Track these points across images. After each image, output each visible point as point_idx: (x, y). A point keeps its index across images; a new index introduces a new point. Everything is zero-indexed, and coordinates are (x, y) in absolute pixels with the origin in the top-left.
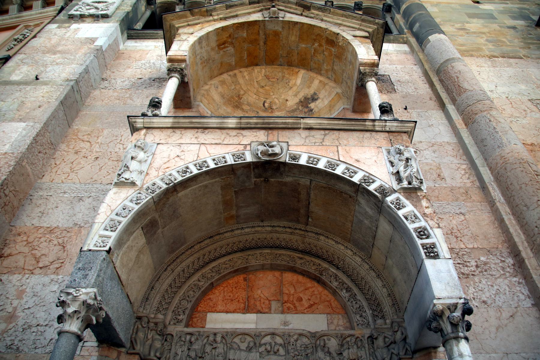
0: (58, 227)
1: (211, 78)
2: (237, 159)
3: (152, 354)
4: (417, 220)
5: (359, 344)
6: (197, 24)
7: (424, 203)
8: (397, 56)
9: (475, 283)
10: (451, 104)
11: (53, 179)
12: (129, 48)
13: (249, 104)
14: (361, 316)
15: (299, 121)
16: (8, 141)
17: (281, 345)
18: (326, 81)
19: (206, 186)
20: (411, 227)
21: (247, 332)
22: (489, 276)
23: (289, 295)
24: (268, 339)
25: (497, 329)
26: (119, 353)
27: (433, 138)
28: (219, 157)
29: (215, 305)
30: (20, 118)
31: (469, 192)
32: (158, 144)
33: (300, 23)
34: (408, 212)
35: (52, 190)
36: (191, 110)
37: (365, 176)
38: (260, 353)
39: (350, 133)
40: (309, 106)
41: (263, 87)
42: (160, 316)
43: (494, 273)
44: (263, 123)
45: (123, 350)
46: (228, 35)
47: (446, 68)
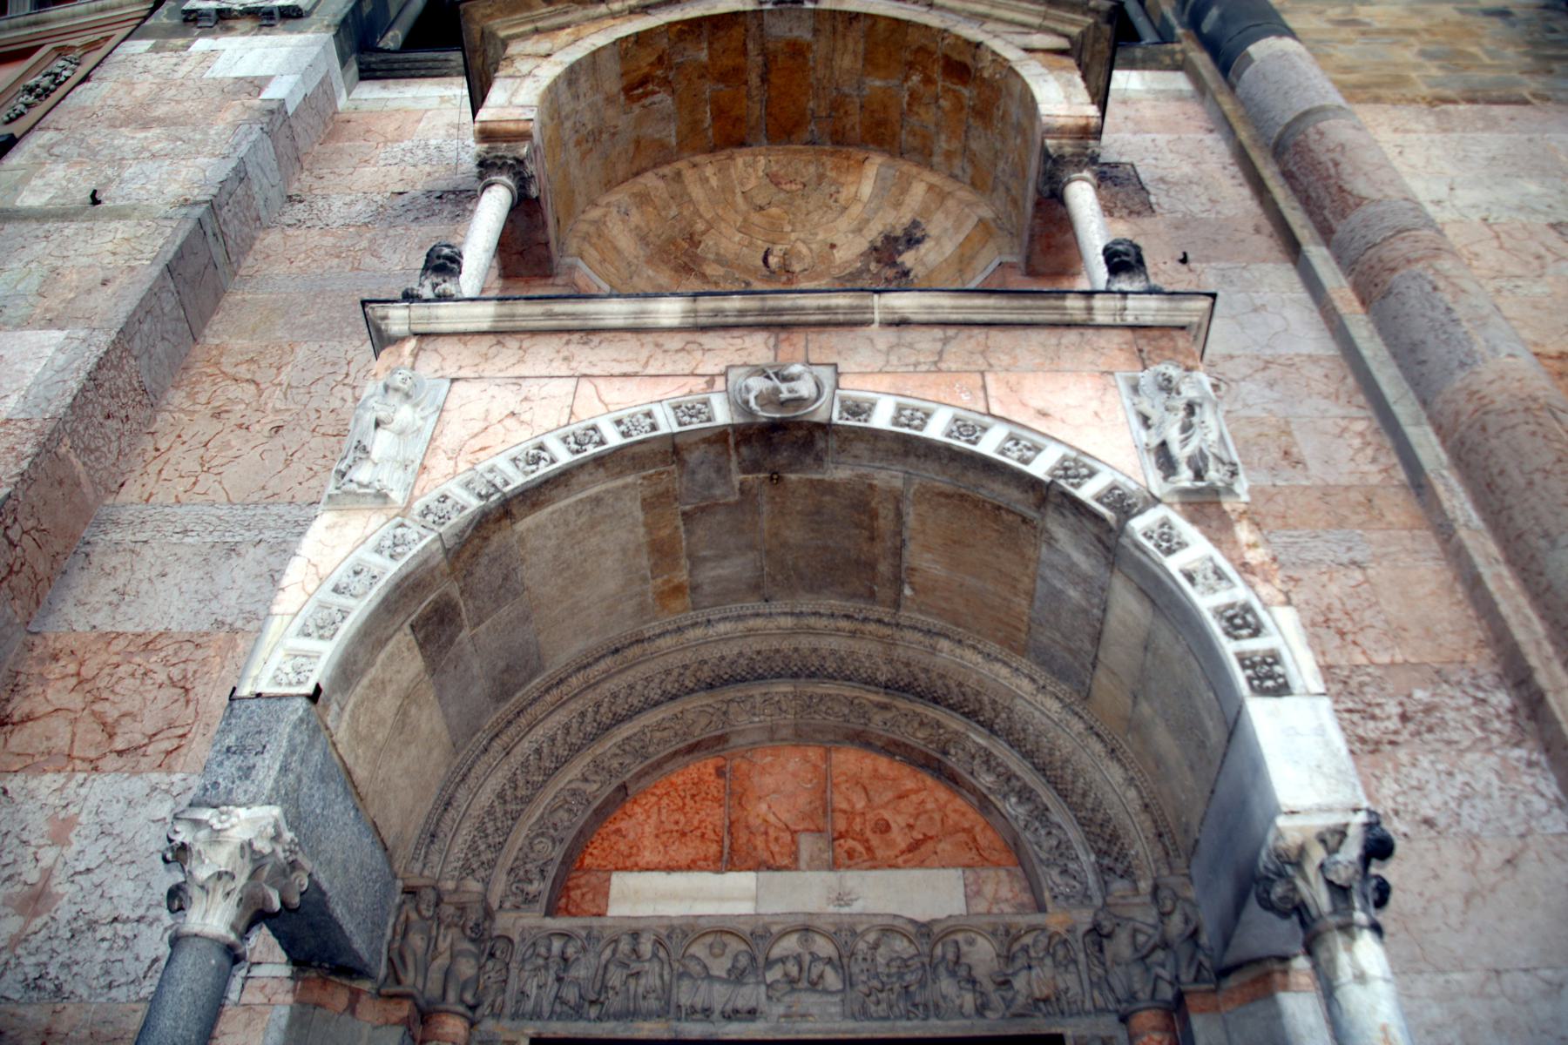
0: (165, 633)
1: (609, 185)
2: (687, 419)
3: (452, 996)
4: (1224, 584)
5: (1061, 953)
6: (561, 27)
7: (1244, 533)
8: (1154, 107)
9: (1397, 766)
10: (1317, 244)
11: (151, 495)
12: (365, 107)
13: (720, 260)
14: (1064, 871)
15: (866, 302)
16: (15, 386)
17: (829, 961)
18: (949, 186)
19: (597, 501)
20: (1206, 602)
21: (728, 925)
22: (1438, 746)
23: (850, 815)
24: (791, 944)
25: (1468, 900)
26: (355, 995)
27: (1268, 346)
28: (633, 416)
30: (48, 316)
31: (1377, 501)
32: (453, 380)
33: (867, 15)
35: (149, 526)
36: (550, 281)
37: (1065, 458)
38: (769, 986)
39: (1019, 333)
40: (899, 260)
41: (762, 208)
42: (474, 886)
43: (1455, 736)
45: (366, 985)
46: (653, 58)
47: (1301, 137)
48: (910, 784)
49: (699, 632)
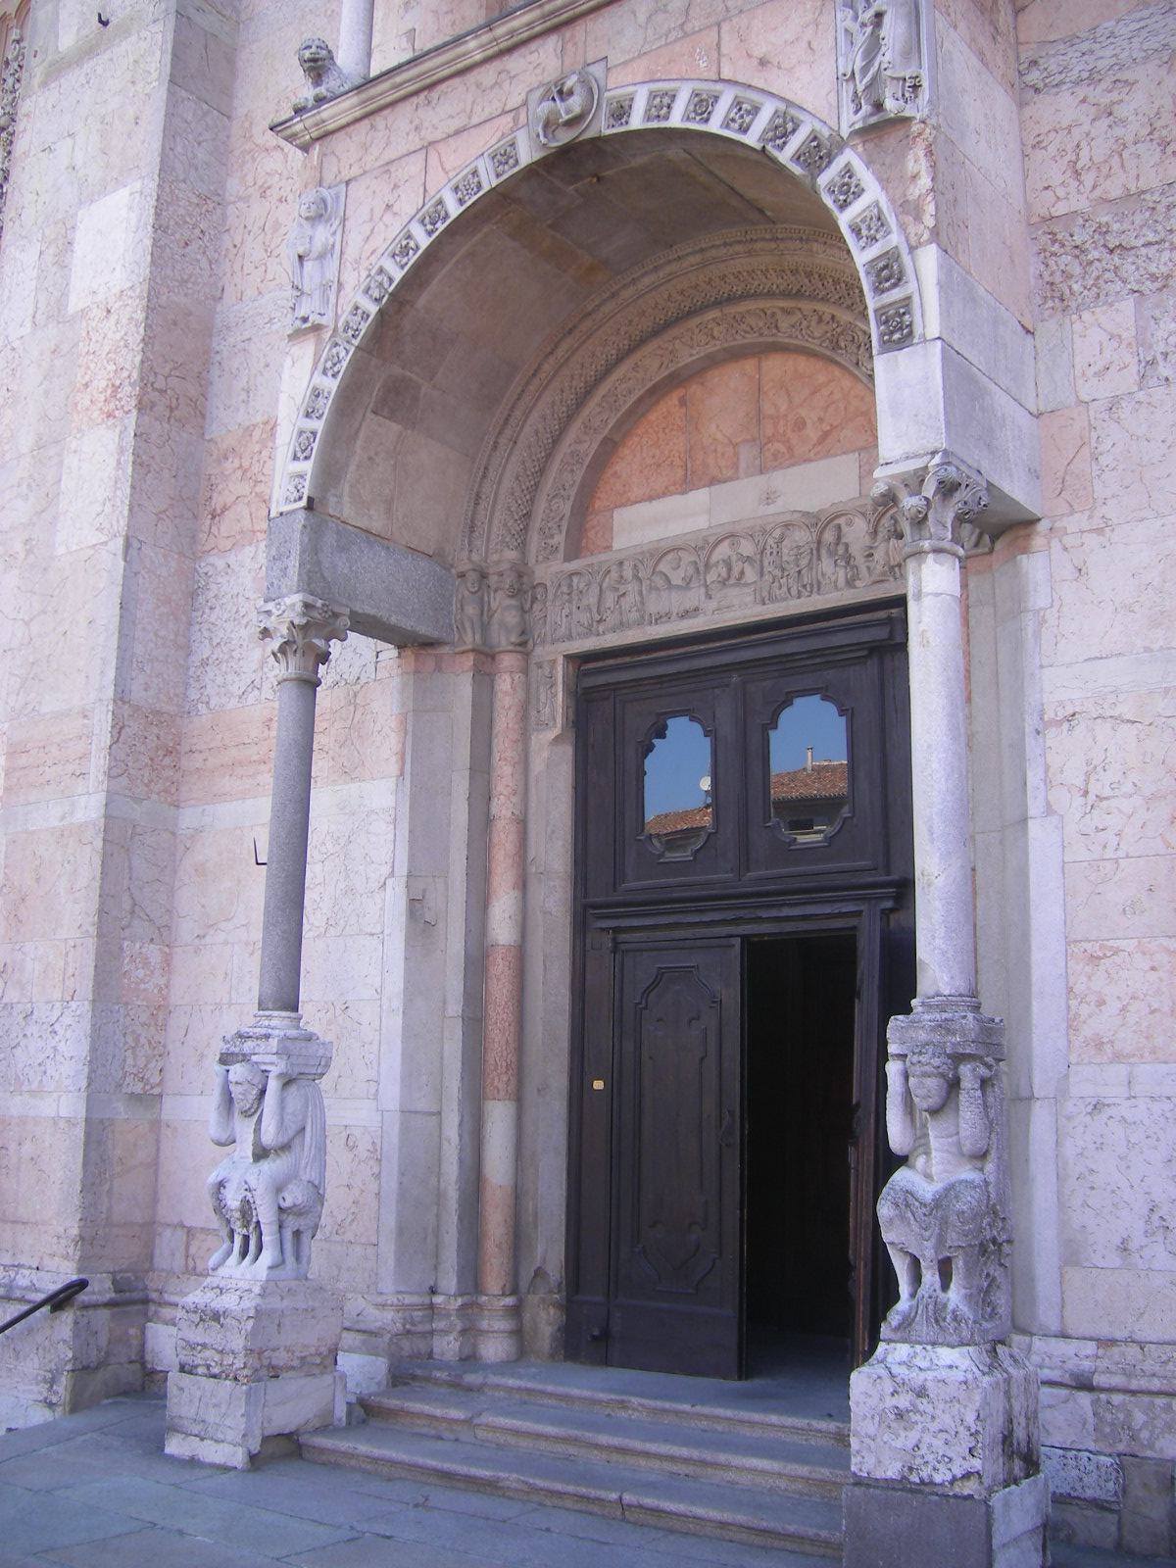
19: (472, 254)
24: (724, 550)
29: (627, 489)
34: (864, 211)
44: (545, 17)
48: (821, 378)
49: (630, 291)
